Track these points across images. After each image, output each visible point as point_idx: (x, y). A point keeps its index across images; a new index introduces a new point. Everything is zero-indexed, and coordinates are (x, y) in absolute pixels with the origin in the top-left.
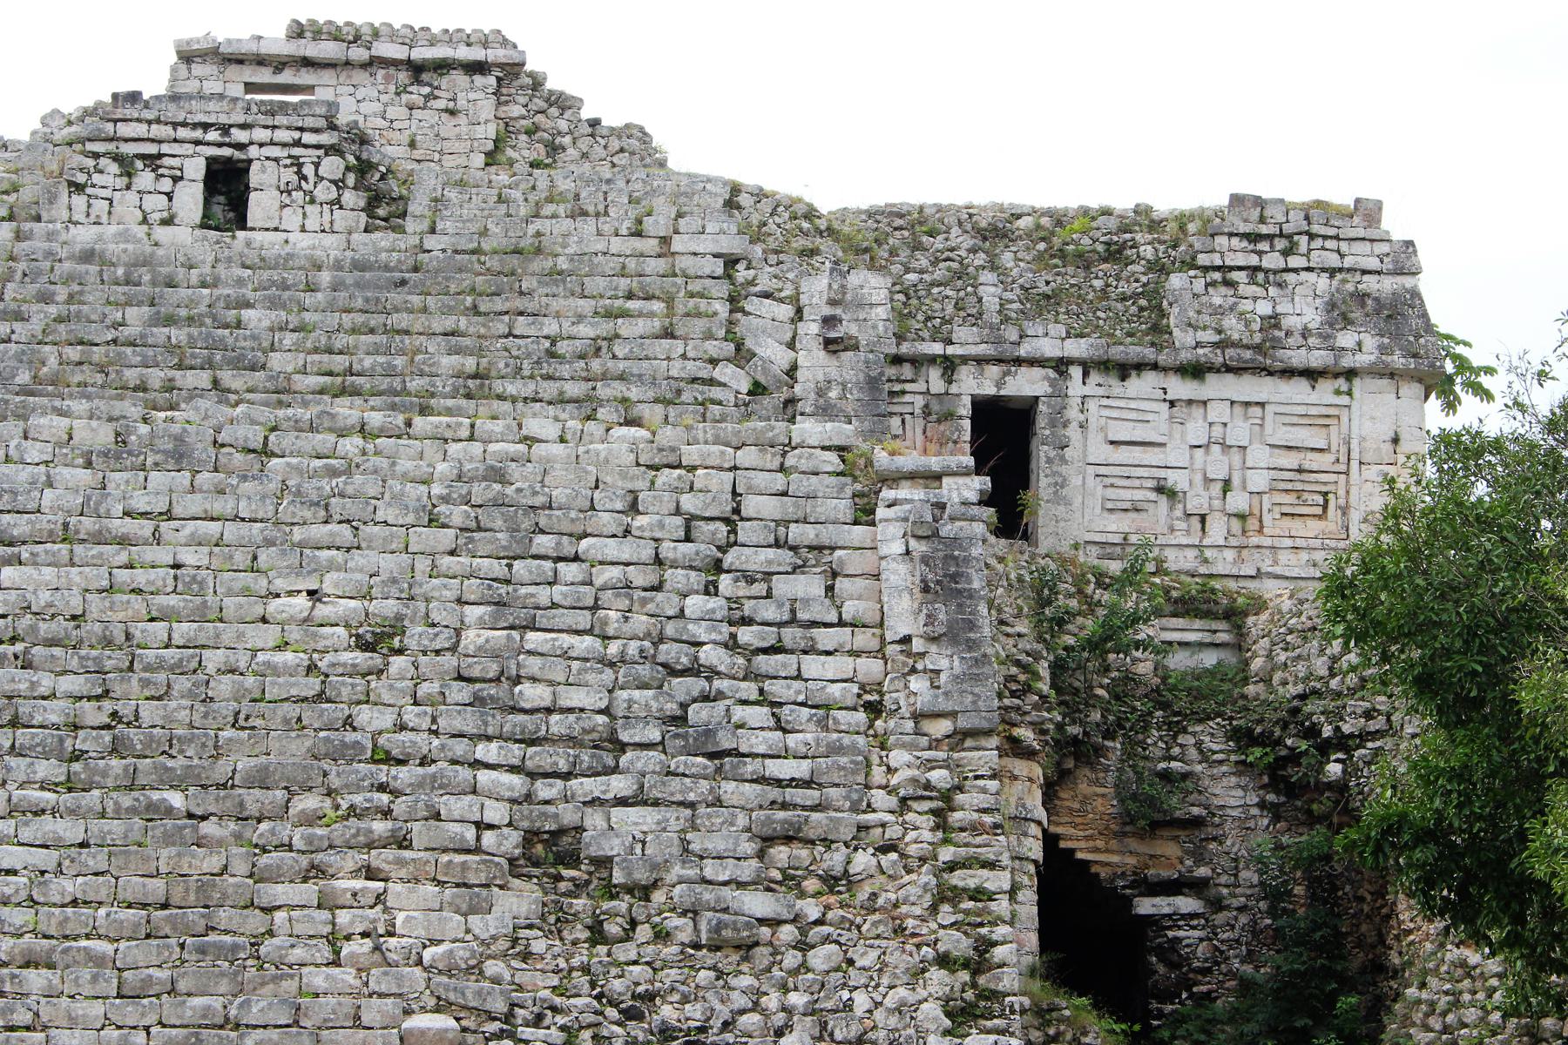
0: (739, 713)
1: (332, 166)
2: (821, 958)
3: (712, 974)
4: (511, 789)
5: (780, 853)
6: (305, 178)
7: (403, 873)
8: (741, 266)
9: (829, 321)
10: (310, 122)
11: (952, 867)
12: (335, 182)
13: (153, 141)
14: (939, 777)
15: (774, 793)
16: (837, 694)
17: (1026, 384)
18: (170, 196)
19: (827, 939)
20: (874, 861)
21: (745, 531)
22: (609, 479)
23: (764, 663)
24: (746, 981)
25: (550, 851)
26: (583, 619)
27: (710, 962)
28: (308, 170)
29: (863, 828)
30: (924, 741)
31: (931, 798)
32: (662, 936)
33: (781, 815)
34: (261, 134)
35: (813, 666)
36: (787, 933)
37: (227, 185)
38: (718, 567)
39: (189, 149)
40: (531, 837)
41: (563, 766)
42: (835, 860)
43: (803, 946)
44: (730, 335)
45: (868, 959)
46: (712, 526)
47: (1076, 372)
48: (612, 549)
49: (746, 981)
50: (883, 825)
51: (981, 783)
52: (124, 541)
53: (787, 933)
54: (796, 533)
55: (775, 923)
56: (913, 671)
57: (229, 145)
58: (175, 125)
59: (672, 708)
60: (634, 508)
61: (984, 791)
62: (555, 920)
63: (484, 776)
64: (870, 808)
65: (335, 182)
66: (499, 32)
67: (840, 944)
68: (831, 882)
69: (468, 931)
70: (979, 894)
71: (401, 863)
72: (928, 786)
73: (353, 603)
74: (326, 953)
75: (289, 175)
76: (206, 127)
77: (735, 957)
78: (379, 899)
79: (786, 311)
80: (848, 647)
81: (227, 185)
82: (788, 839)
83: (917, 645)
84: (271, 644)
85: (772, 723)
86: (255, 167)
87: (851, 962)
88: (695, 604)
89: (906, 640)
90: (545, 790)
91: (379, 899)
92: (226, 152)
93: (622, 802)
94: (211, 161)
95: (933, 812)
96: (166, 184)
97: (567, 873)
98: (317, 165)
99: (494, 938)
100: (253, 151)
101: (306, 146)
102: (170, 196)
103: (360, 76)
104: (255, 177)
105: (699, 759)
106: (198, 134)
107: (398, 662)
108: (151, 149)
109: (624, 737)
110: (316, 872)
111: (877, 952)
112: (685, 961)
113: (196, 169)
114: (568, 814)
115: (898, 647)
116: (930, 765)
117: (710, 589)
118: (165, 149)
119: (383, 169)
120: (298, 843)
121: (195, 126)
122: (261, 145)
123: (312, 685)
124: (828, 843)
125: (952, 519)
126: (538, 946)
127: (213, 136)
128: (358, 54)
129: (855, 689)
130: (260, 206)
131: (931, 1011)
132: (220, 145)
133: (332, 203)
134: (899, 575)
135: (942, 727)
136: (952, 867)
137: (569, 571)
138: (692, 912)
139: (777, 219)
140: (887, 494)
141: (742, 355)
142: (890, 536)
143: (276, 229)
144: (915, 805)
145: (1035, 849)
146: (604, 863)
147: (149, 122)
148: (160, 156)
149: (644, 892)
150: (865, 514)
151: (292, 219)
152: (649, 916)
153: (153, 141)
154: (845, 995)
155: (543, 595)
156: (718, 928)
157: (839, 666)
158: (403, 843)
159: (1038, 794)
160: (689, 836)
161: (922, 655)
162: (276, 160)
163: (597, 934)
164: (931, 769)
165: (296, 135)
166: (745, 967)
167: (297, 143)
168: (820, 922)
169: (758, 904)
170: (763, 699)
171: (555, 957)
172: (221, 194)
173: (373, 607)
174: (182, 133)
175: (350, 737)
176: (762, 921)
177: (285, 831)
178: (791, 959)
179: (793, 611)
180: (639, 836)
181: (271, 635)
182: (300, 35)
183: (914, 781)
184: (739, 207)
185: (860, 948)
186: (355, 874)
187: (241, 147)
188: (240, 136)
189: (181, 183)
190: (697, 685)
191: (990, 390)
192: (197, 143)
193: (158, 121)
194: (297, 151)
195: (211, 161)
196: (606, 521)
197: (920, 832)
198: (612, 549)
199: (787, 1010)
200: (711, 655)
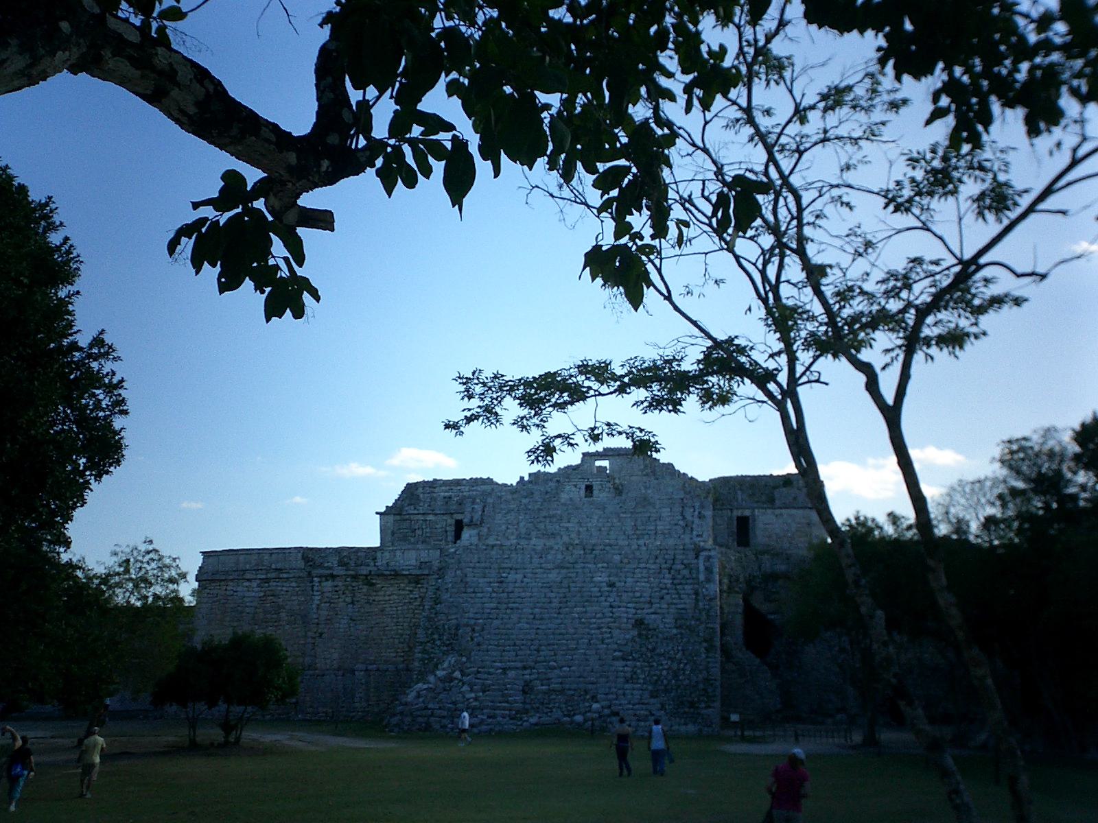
1: (609, 485)
2: (684, 640)
9: (699, 513)
14: (707, 607)
17: (747, 513)
21: (676, 562)
23: (678, 587)
25: (639, 623)
26: (646, 580)
35: (686, 587)
36: (679, 636)
37: (589, 489)
38: (671, 568)
40: (636, 620)
43: (682, 638)
44: (682, 514)
47: (756, 511)
48: (653, 567)
52: (568, 568)
54: (685, 562)
60: (657, 558)
62: (640, 635)
63: (629, 610)
78: (610, 632)
79: (692, 510)
81: (589, 489)
88: (667, 576)
90: (639, 611)
107: (615, 589)
110: (599, 628)
113: (583, 487)
117: (669, 573)
123: (599, 594)
130: (595, 492)
131: (703, 650)
134: (702, 568)
135: (707, 598)
137: (645, 571)
140: (701, 554)
141: (684, 518)
145: (740, 610)
146: (648, 624)
149: (655, 630)
150: (697, 558)
155: (640, 575)
158: (615, 622)
159: (741, 600)
169: (675, 631)
177: (594, 620)
181: (592, 585)
190: (665, 591)
191: (739, 514)
196: (651, 561)
198: (653, 567)
199: (678, 650)
200: (669, 586)
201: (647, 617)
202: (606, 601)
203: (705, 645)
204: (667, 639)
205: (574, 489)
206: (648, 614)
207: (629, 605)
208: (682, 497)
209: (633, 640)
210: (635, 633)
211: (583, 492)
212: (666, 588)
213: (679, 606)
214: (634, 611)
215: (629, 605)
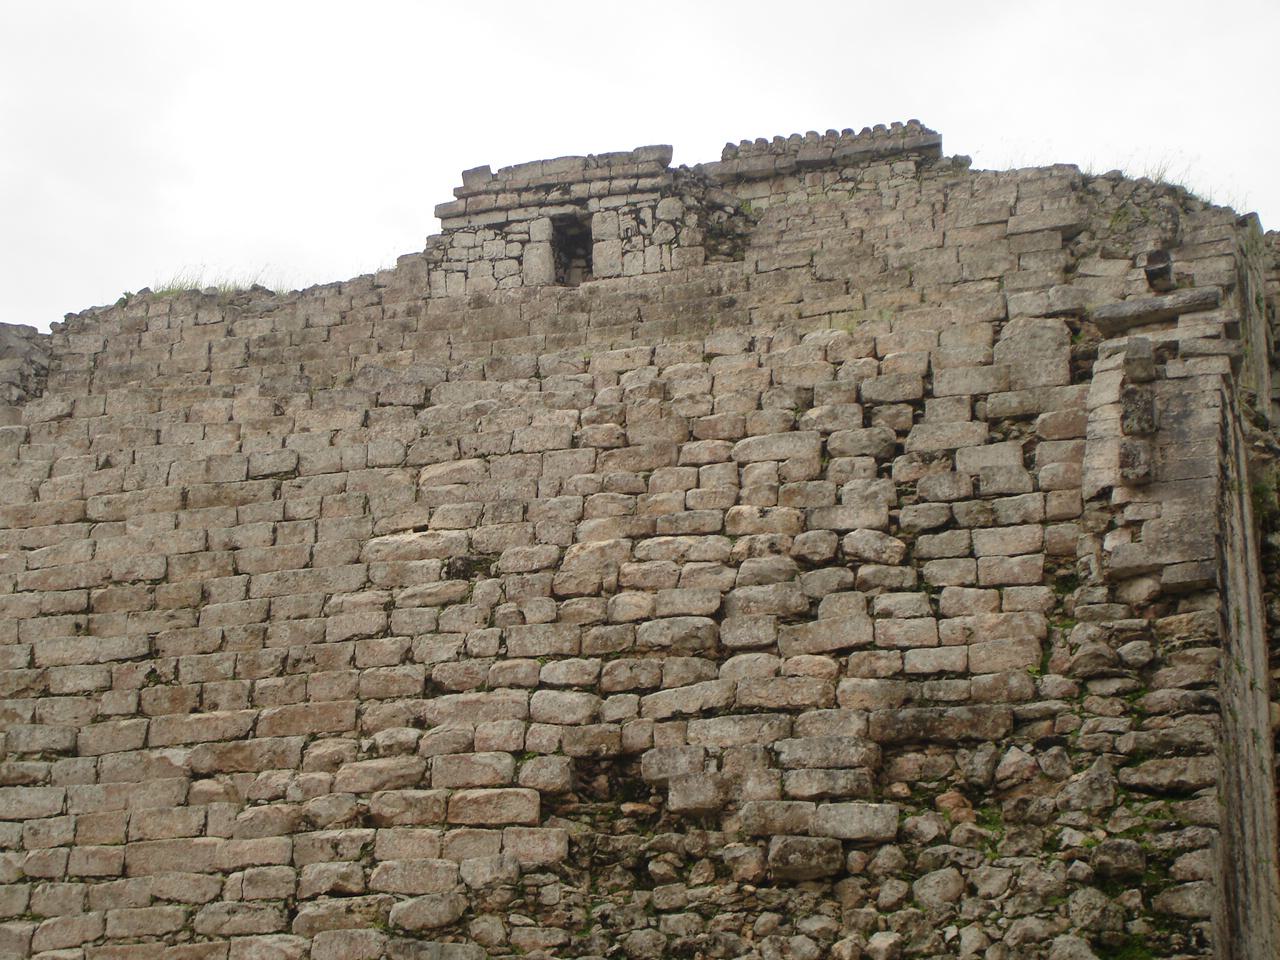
0: (884, 601)
2: (934, 888)
3: (775, 917)
4: (572, 709)
5: (910, 762)
6: (643, 222)
7: (408, 817)
8: (1083, 238)
10: (643, 168)
11: (1134, 758)
12: (672, 222)
13: (499, 209)
15: (902, 688)
16: (1016, 570)
18: (519, 259)
19: (939, 863)
20: (1031, 761)
22: (785, 378)
23: (925, 544)
24: (814, 924)
25: (608, 778)
27: (776, 902)
28: (646, 215)
29: (1019, 722)
30: (1120, 609)
31: (1121, 676)
32: (723, 871)
33: (908, 712)
34: (597, 187)
37: (572, 244)
39: (534, 211)
41: (645, 680)
42: (977, 763)
43: (911, 872)
45: (992, 882)
46: (894, 409)
49: (814, 924)
50: (1052, 715)
51: (1191, 652)
53: (887, 856)
55: (869, 844)
56: (1111, 526)
57: (571, 202)
58: (519, 191)
59: (796, 601)
61: (1194, 660)
62: (585, 862)
64: (1037, 696)
65: (672, 222)
66: (915, 122)
67: (959, 867)
68: (973, 793)
69: (460, 881)
70: (1179, 792)
71: (410, 804)
72: (1119, 661)
73: (455, 533)
74: (271, 916)
75: (629, 222)
76: (548, 188)
77: (812, 893)
80: (1038, 516)
81: (572, 244)
82: (922, 745)
83: (1117, 497)
84: (355, 585)
85: (927, 608)
86: (596, 218)
87: (972, 890)
89: (1105, 493)
91: (367, 849)
92: (569, 209)
93: (708, 713)
94: (553, 219)
95: (1117, 694)
96: (515, 249)
97: (627, 807)
98: (654, 208)
99: (489, 886)
100: (593, 204)
101: (642, 191)
102: (519, 259)
103: (790, 183)
104: (597, 227)
105: (824, 658)
106: (542, 195)
108: (500, 218)
109: (729, 638)
111: (1006, 874)
112: (748, 907)
113: (541, 229)
114: (636, 735)
115: (1096, 505)
116: (1121, 636)
118: (513, 215)
119: (730, 210)
120: (295, 794)
121: (538, 189)
122: (600, 197)
124: (972, 743)
125: (1186, 356)
126: (552, 893)
127: (555, 195)
128: (782, 163)
129: (1040, 560)
130: (604, 254)
132: (562, 204)
133: (670, 243)
135: (1142, 589)
136: (1134, 758)
138: (759, 837)
139: (1138, 200)
142: (1106, 386)
143: (618, 276)
144: (1096, 687)
147: (497, 193)
148: (508, 223)
149: (712, 817)
150: (1080, 371)
151: (634, 265)
152: (706, 847)
153: (499, 209)
154: (951, 931)
156: (782, 857)
157: (1031, 534)
160: (777, 745)
161: (1122, 507)
162: (616, 209)
163: (643, 879)
164: (1125, 641)
165: (633, 182)
166: (827, 906)
167: (634, 190)
168: (942, 839)
170: (921, 584)
171: (569, 907)
172: (579, 257)
173: (475, 534)
174: (527, 197)
175: (408, 668)
176: (849, 844)
178: (890, 891)
179: (976, 486)
180: (713, 747)
182: (735, 156)
183: (1097, 656)
184: (1095, 193)
185: (984, 870)
186: (351, 822)
187: (582, 202)
188: (578, 190)
189: (528, 246)
192: (541, 204)
193: (504, 191)
194: (634, 198)
195: (553, 219)
197: (1103, 717)
200: (861, 541)
201: (670, 735)
202: (407, 657)
203: (1085, 902)
204: (789, 880)
205: (495, 247)
206: (678, 716)
207: (556, 672)
208: (1070, 218)
209: (522, 895)
210: (548, 844)
211: (539, 260)
212: (837, 559)
213: (918, 661)
214: (576, 704)
215: (556, 672)
